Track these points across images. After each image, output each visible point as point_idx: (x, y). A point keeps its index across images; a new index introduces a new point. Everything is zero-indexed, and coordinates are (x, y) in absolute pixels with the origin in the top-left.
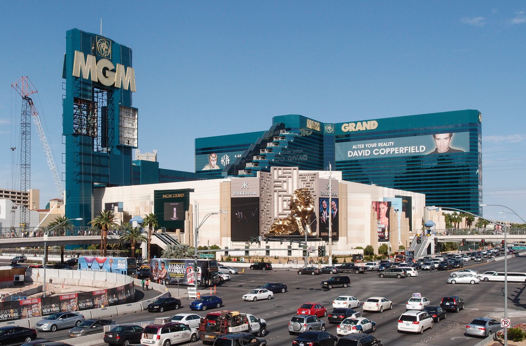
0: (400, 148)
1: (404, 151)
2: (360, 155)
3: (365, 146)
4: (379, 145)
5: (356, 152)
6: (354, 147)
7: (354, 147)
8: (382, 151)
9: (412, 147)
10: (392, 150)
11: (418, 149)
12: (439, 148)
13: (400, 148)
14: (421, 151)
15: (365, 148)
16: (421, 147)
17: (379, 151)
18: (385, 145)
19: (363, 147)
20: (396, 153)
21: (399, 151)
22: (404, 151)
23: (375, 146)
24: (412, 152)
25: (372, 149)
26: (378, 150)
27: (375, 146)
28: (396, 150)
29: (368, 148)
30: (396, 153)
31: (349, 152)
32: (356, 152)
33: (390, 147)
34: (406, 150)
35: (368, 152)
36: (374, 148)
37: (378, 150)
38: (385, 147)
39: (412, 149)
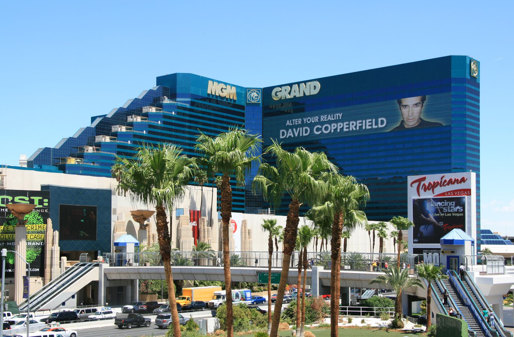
0: (351, 123)
1: (356, 127)
2: (296, 135)
3: (303, 121)
4: (322, 119)
5: (290, 130)
6: (288, 123)
7: (288, 123)
8: (326, 128)
9: (368, 121)
10: (340, 126)
11: (376, 124)
12: (405, 119)
13: (351, 123)
14: (380, 126)
15: (303, 125)
16: (380, 119)
17: (321, 129)
18: (330, 118)
19: (300, 122)
20: (345, 130)
21: (349, 128)
22: (356, 127)
23: (317, 120)
24: (368, 127)
25: (311, 126)
26: (320, 127)
27: (317, 120)
28: (345, 126)
29: (307, 125)
30: (345, 130)
31: (281, 131)
32: (290, 130)
33: (336, 122)
34: (358, 125)
35: (306, 131)
36: (316, 124)
37: (320, 127)
38: (330, 122)
39: (368, 124)
